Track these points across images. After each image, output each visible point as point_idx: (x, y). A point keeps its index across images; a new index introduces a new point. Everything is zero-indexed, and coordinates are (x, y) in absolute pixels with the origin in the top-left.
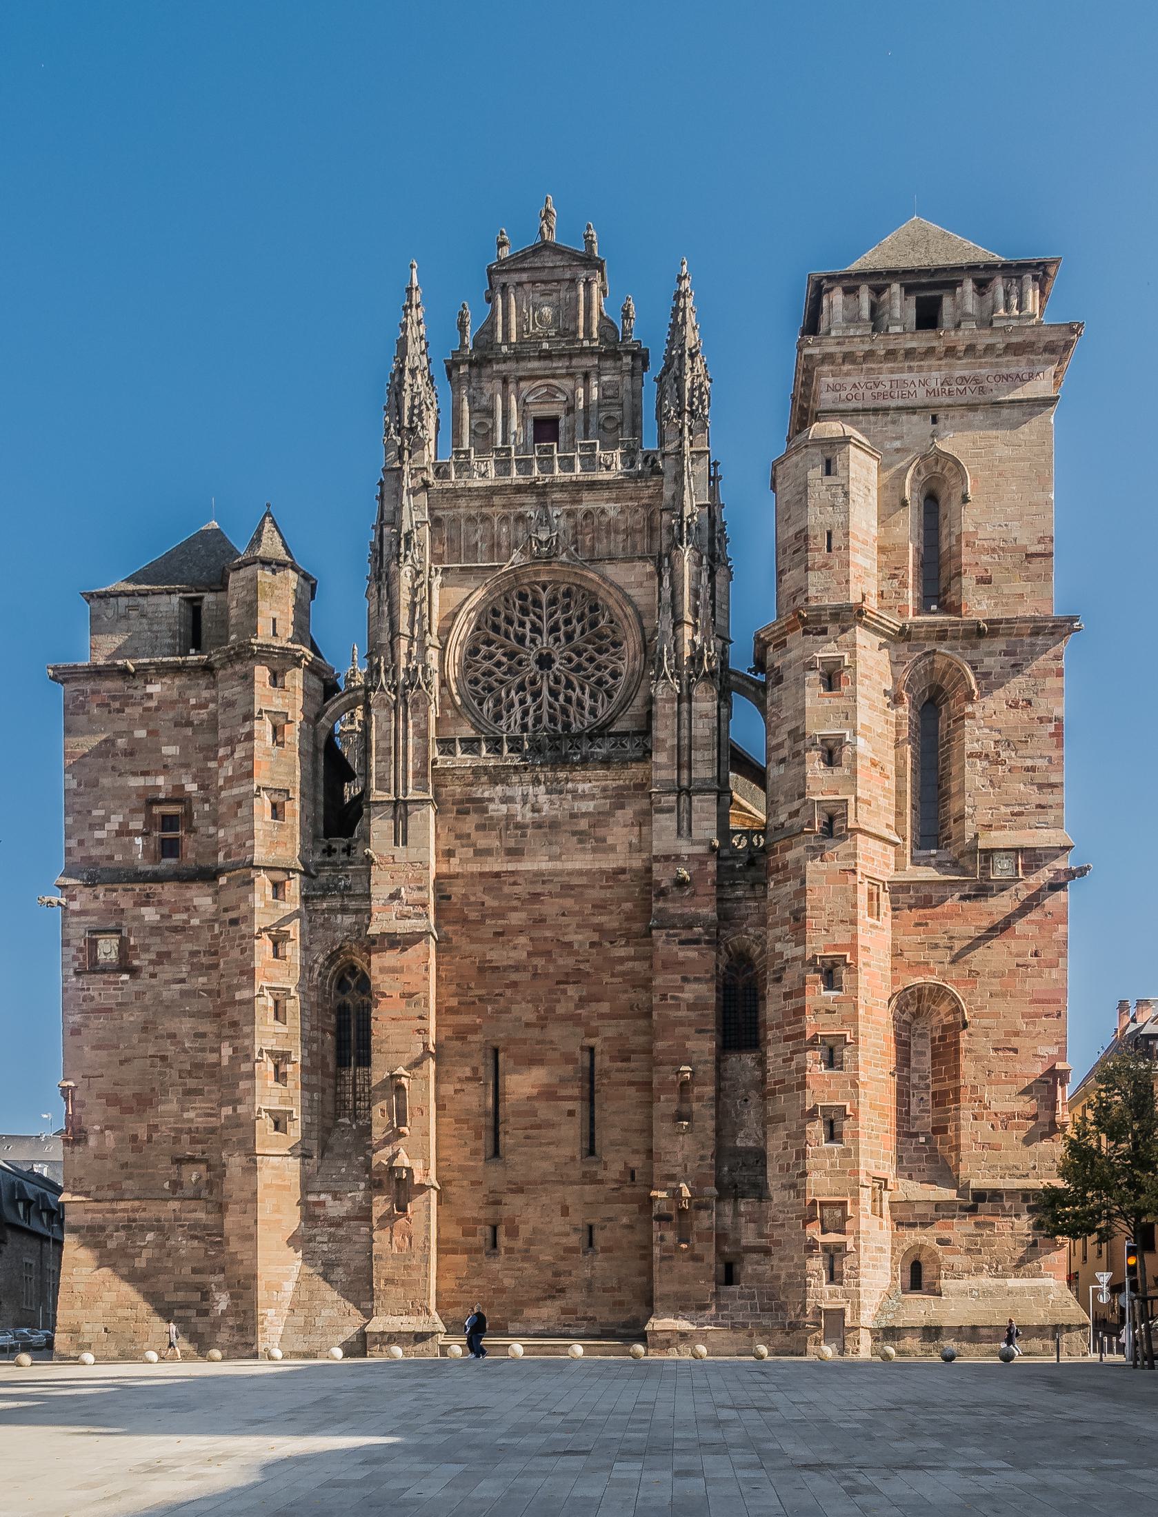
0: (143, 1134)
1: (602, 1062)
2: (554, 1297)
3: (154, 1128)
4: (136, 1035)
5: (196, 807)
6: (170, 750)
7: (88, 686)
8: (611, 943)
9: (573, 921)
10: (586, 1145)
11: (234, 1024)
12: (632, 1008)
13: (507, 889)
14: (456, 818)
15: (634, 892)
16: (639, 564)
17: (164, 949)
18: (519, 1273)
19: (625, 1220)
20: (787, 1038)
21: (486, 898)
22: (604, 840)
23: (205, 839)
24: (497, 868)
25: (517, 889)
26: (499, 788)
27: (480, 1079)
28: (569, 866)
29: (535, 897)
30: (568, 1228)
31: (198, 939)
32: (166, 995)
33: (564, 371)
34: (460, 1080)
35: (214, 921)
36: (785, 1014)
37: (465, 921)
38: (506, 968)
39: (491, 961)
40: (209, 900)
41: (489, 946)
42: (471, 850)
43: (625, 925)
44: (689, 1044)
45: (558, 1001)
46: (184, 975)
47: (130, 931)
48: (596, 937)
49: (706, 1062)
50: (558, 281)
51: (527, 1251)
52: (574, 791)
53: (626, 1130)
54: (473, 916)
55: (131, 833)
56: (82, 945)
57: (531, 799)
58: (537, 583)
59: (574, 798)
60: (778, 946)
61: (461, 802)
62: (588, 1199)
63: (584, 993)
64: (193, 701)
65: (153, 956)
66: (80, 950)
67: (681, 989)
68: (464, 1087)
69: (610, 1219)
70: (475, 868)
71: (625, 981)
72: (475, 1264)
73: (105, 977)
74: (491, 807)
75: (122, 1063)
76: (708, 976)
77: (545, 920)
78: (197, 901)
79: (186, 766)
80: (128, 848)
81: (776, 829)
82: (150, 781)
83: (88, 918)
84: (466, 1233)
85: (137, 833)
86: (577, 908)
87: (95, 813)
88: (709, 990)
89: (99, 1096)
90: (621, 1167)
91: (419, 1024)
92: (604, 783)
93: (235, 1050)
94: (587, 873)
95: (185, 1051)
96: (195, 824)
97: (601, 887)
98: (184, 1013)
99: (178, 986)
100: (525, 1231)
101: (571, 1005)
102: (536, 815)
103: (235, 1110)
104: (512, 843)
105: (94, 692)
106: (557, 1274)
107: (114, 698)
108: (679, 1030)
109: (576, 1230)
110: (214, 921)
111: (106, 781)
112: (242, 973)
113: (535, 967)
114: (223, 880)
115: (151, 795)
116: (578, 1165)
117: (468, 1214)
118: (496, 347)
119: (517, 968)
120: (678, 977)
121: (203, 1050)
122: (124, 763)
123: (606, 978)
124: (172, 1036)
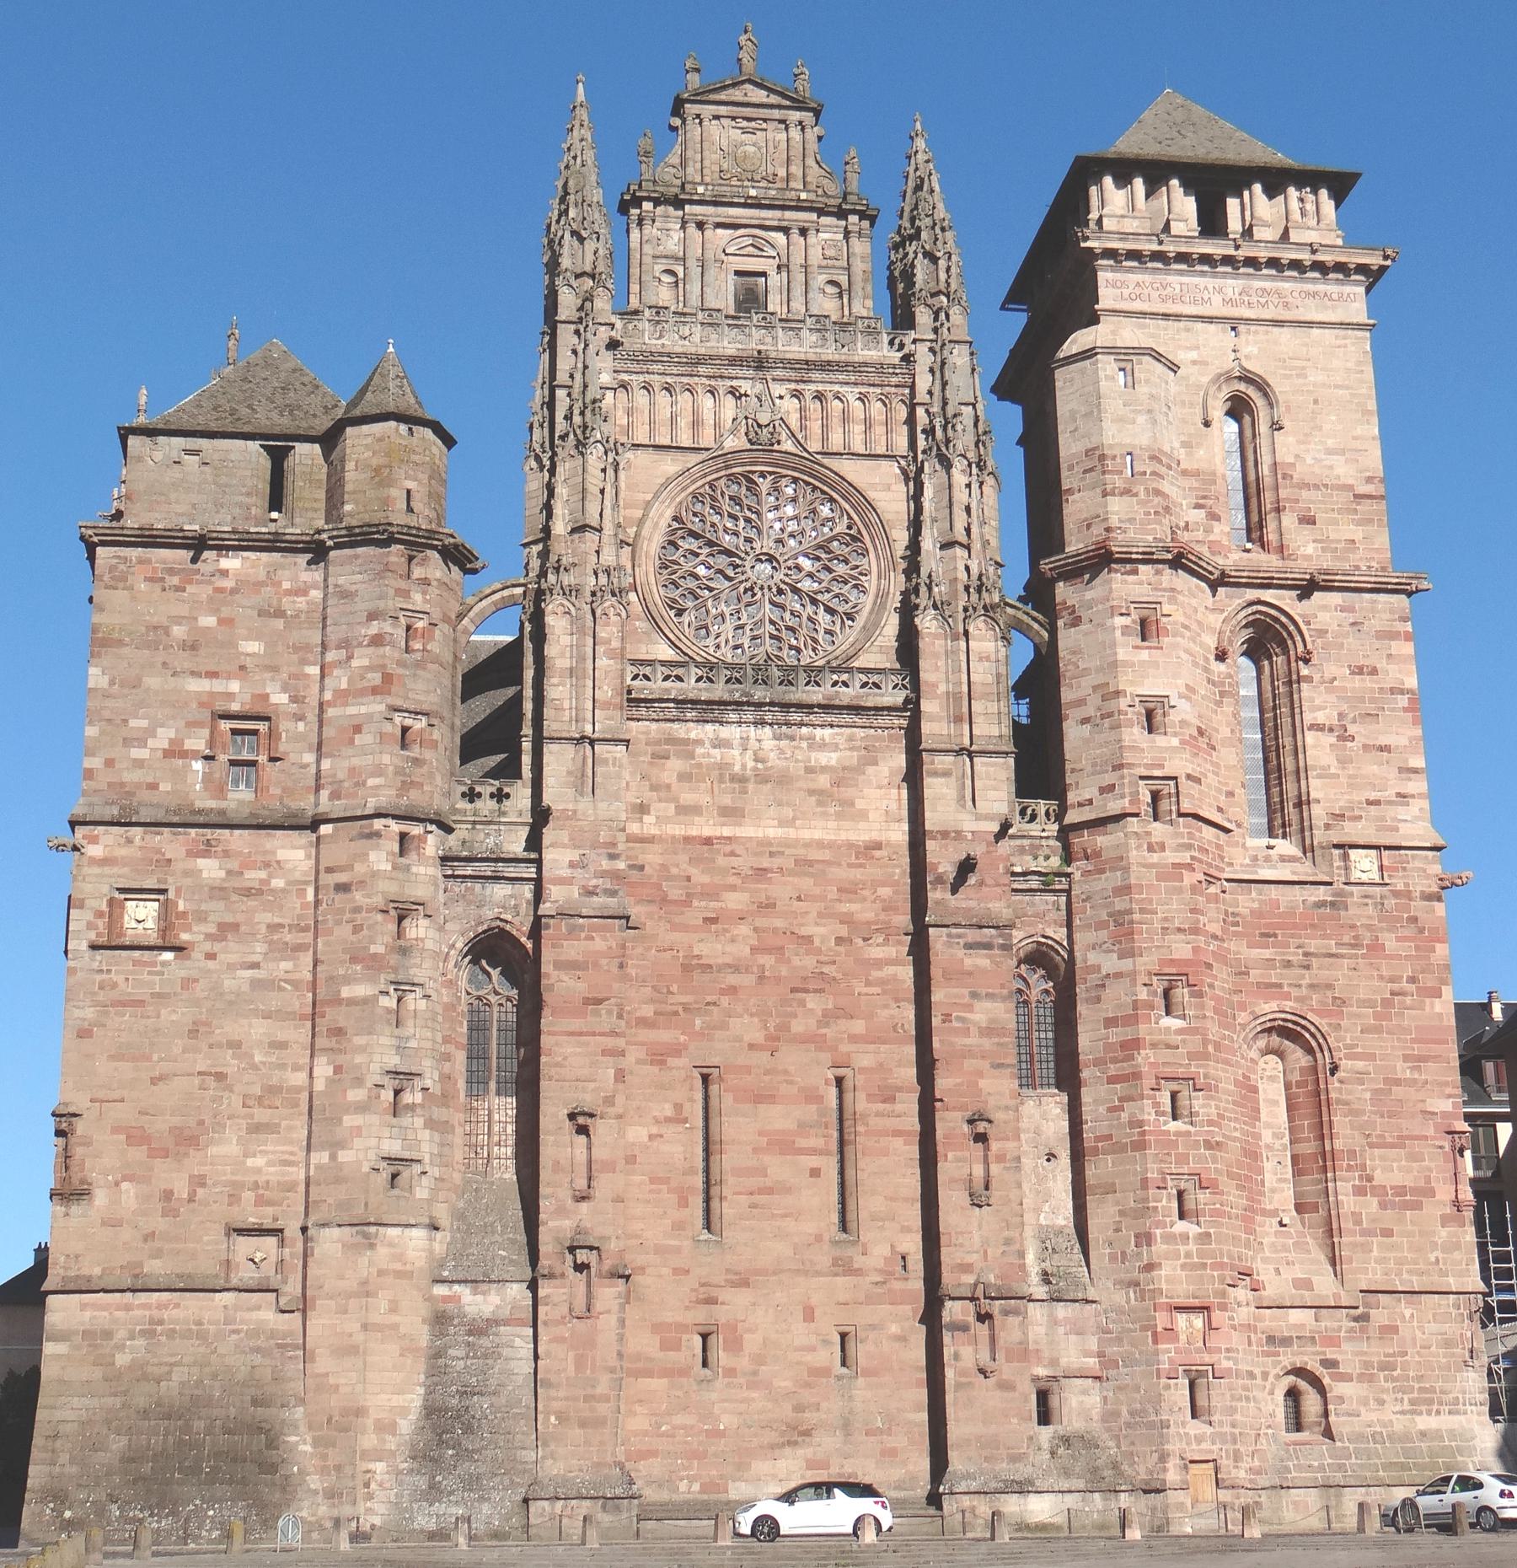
0: (182, 1190)
1: (860, 1103)
2: (796, 1443)
3: (200, 1181)
4: (179, 1042)
5: (285, 726)
6: (253, 647)
7: (134, 553)
8: (865, 940)
9: (813, 908)
10: (835, 1218)
11: (338, 1032)
12: (895, 1030)
13: (721, 861)
14: (651, 763)
15: (894, 874)
16: (884, 463)
17: (229, 919)
18: (743, 1407)
19: (894, 1329)
20: (1112, 1080)
21: (693, 871)
22: (852, 804)
23: (294, 770)
24: (707, 832)
25: (735, 862)
26: (709, 727)
27: (685, 1121)
28: (806, 834)
29: (761, 873)
30: (813, 1339)
31: (281, 907)
32: (228, 984)
33: (775, 223)
34: (657, 1121)
35: (307, 883)
36: (1108, 1047)
37: (664, 900)
38: (722, 968)
39: (699, 957)
40: (301, 854)
41: (696, 937)
42: (673, 806)
43: (882, 917)
44: (982, 1083)
45: (796, 1016)
46: (257, 958)
47: (178, 891)
48: (843, 931)
49: (1007, 1108)
50: (765, 120)
51: (755, 1373)
52: (811, 738)
53: (892, 1199)
54: (675, 893)
55: (185, 754)
56: (104, 907)
57: (753, 744)
58: (753, 472)
59: (810, 747)
60: (1093, 958)
61: (658, 742)
62: (841, 1300)
63: (830, 1006)
64: (286, 585)
65: (212, 929)
66: (100, 914)
67: (969, 1008)
68: (663, 1130)
69: (873, 1327)
70: (677, 830)
71: (885, 992)
72: (680, 1393)
73: (137, 954)
74: (699, 751)
75: (154, 1081)
76: (1005, 992)
77: (774, 905)
78: (282, 854)
79: (275, 669)
80: (181, 775)
81: (1080, 805)
82: (218, 686)
83: (115, 870)
84: (665, 1346)
85: (194, 755)
86: (817, 891)
87: (133, 723)
88: (1007, 1012)
89: (116, 1130)
90: (887, 1252)
91: (610, 1042)
92: (849, 730)
93: (338, 1069)
94: (830, 845)
95: (255, 1067)
96: (283, 747)
97: (850, 865)
98: (255, 1013)
99: (249, 973)
100: (751, 1342)
101: (812, 1023)
102: (760, 766)
103: (333, 1157)
104: (727, 800)
105: (141, 561)
106: (799, 1408)
107: (171, 571)
108: (970, 1064)
109: (826, 1342)
110: (307, 883)
111: (153, 682)
112: (354, 960)
113: (762, 968)
114: (325, 829)
115: (220, 706)
116: (826, 1247)
117: (669, 1317)
118: (688, 187)
119: (736, 968)
120: (966, 992)
121: (283, 1066)
122: (182, 660)
123: (859, 988)
124: (235, 1045)
